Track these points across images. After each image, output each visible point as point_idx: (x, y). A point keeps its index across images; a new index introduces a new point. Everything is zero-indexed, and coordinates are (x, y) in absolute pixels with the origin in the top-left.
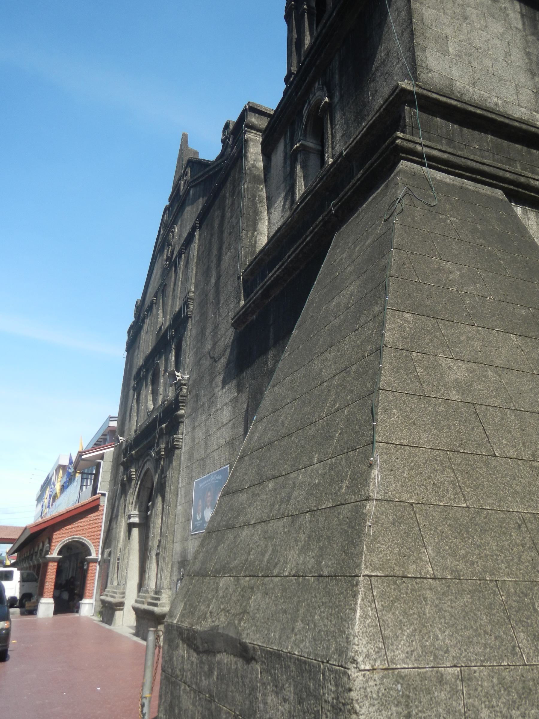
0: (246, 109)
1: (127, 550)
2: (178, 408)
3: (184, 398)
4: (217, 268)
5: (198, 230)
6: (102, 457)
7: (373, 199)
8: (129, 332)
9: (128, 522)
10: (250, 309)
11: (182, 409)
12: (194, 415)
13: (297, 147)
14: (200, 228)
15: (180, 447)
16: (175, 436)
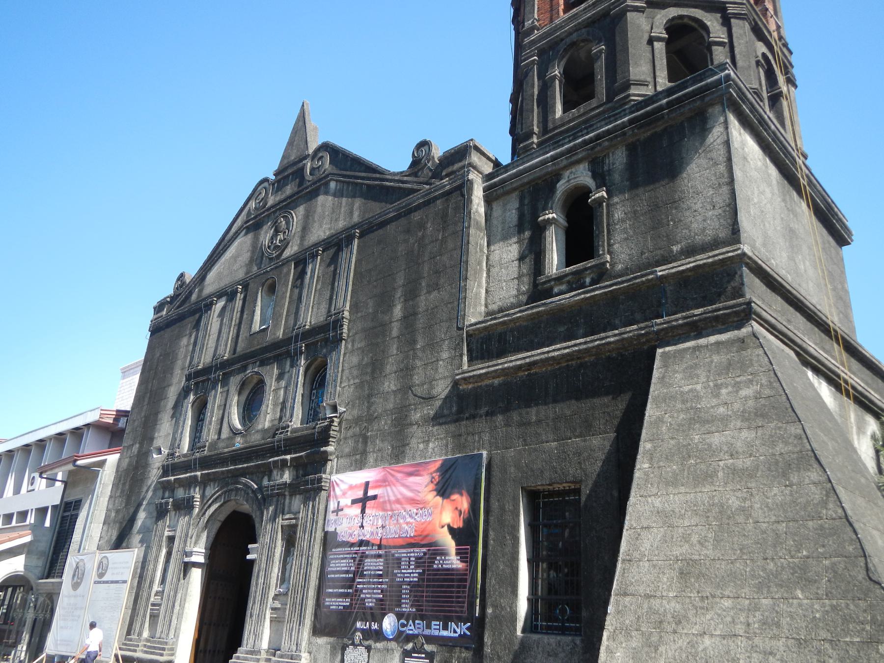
0: (470, 146)
1: (179, 596)
2: (327, 444)
3: (336, 433)
4: (405, 300)
5: (356, 240)
6: (102, 464)
7: (718, 343)
9: (186, 560)
10: (493, 374)
11: (331, 445)
12: (358, 457)
13: (548, 219)
14: (359, 238)
15: (327, 488)
16: (324, 476)
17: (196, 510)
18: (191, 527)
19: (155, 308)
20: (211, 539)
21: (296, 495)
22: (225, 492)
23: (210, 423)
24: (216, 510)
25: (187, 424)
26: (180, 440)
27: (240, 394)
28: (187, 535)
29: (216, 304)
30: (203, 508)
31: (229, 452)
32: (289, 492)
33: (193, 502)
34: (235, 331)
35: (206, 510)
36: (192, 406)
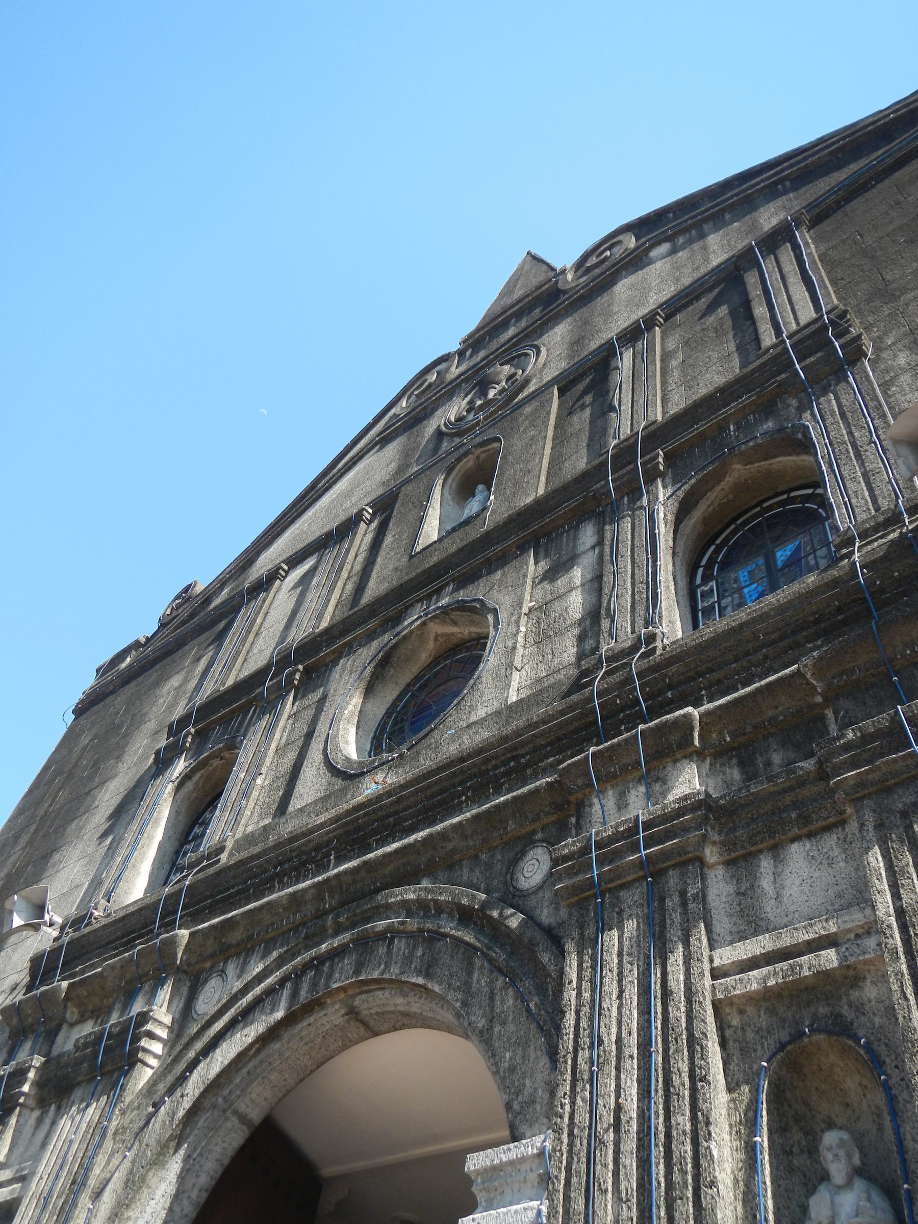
8: (102, 671)
17: (143, 1076)
18: (108, 1144)
19: (98, 671)
20: (204, 1180)
21: (776, 850)
22: (297, 975)
23: (245, 794)
24: (241, 1058)
25: (150, 838)
26: (118, 879)
27: (369, 691)
28: (78, 1184)
29: (285, 578)
30: (176, 1060)
31: (337, 819)
32: (727, 845)
33: (136, 1038)
34: (350, 587)
35: (193, 1065)
36: (178, 789)
